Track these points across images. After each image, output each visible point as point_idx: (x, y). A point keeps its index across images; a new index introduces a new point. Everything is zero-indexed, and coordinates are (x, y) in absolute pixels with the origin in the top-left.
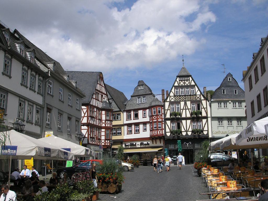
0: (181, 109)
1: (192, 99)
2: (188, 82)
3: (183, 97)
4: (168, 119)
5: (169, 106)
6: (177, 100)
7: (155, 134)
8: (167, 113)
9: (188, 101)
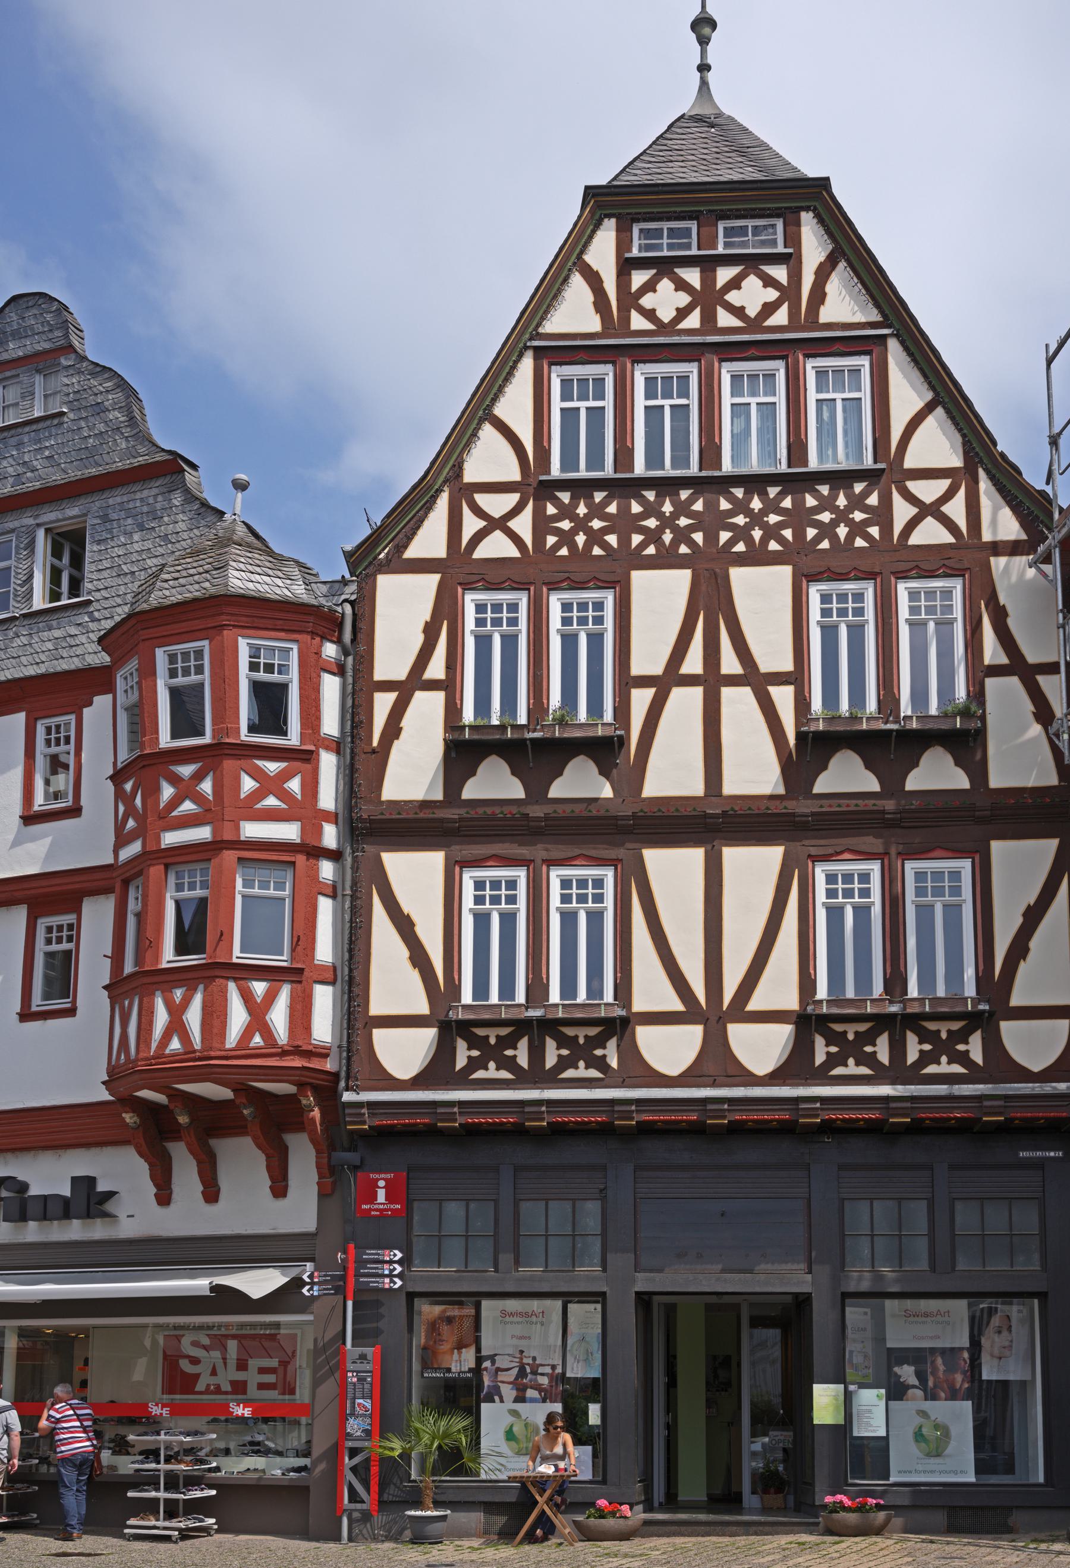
0: (626, 682)
1: (827, 531)
2: (769, 282)
3: (682, 509)
4: (413, 828)
6: (566, 538)
7: (175, 1044)
8: (393, 730)
9: (757, 557)
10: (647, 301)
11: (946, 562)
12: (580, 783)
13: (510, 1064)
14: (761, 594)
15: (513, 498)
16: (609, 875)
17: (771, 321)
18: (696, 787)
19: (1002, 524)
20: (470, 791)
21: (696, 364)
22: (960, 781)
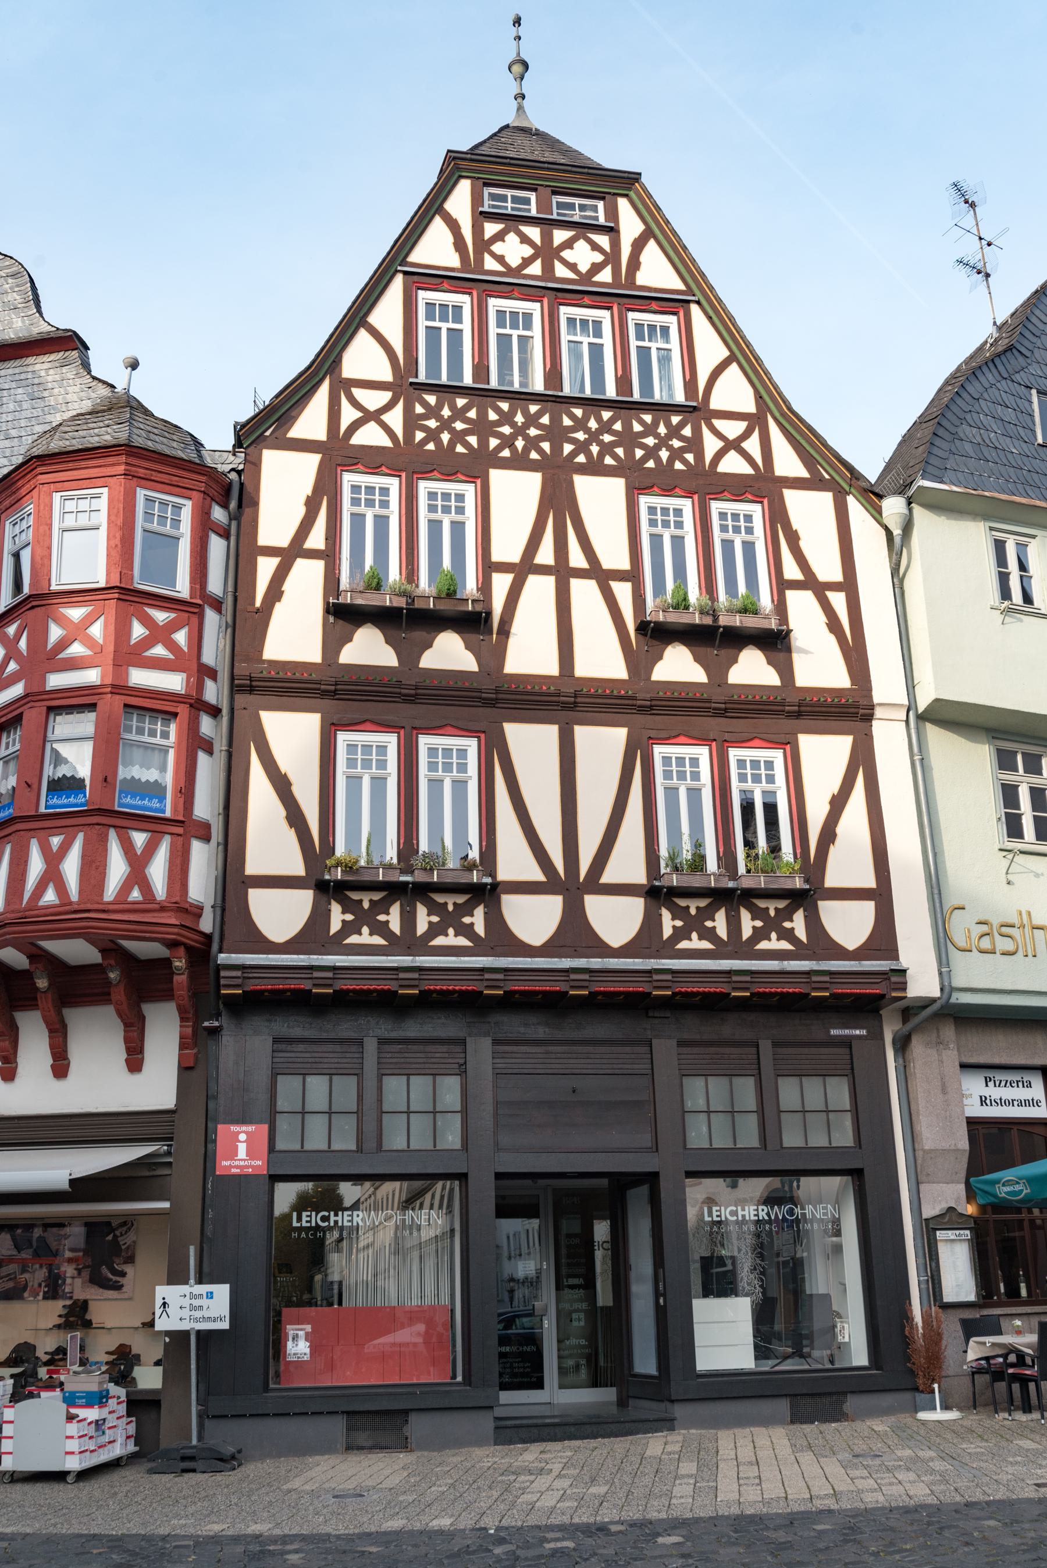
0: (488, 567)
3: (532, 420)
4: (292, 687)
5: (312, 505)
6: (433, 435)
7: (50, 896)
8: (275, 592)
9: (595, 468)
10: (497, 248)
11: (749, 489)
12: (449, 653)
13: (381, 929)
14: (600, 499)
15: (386, 396)
16: (471, 745)
17: (597, 278)
18: (551, 667)
19: (787, 462)
20: (349, 655)
21: (538, 305)
22: (770, 677)
